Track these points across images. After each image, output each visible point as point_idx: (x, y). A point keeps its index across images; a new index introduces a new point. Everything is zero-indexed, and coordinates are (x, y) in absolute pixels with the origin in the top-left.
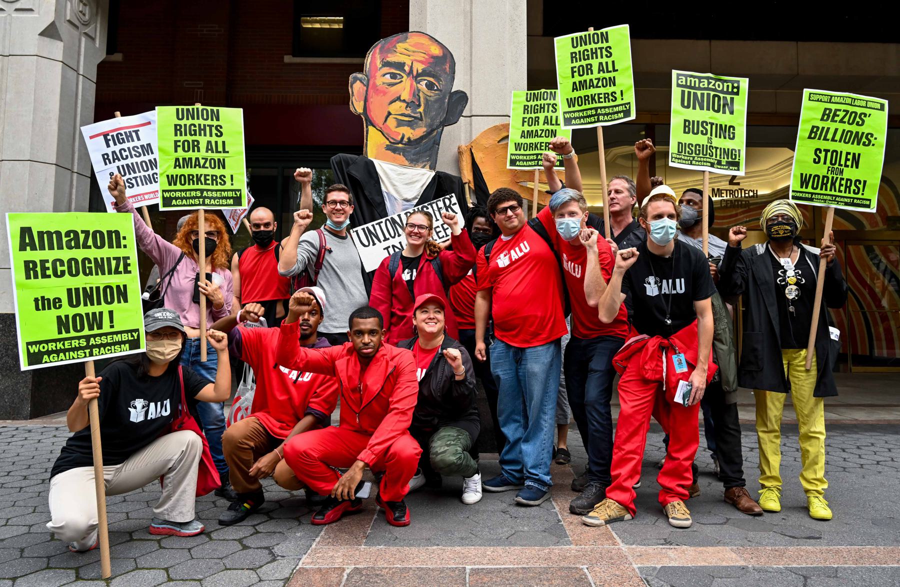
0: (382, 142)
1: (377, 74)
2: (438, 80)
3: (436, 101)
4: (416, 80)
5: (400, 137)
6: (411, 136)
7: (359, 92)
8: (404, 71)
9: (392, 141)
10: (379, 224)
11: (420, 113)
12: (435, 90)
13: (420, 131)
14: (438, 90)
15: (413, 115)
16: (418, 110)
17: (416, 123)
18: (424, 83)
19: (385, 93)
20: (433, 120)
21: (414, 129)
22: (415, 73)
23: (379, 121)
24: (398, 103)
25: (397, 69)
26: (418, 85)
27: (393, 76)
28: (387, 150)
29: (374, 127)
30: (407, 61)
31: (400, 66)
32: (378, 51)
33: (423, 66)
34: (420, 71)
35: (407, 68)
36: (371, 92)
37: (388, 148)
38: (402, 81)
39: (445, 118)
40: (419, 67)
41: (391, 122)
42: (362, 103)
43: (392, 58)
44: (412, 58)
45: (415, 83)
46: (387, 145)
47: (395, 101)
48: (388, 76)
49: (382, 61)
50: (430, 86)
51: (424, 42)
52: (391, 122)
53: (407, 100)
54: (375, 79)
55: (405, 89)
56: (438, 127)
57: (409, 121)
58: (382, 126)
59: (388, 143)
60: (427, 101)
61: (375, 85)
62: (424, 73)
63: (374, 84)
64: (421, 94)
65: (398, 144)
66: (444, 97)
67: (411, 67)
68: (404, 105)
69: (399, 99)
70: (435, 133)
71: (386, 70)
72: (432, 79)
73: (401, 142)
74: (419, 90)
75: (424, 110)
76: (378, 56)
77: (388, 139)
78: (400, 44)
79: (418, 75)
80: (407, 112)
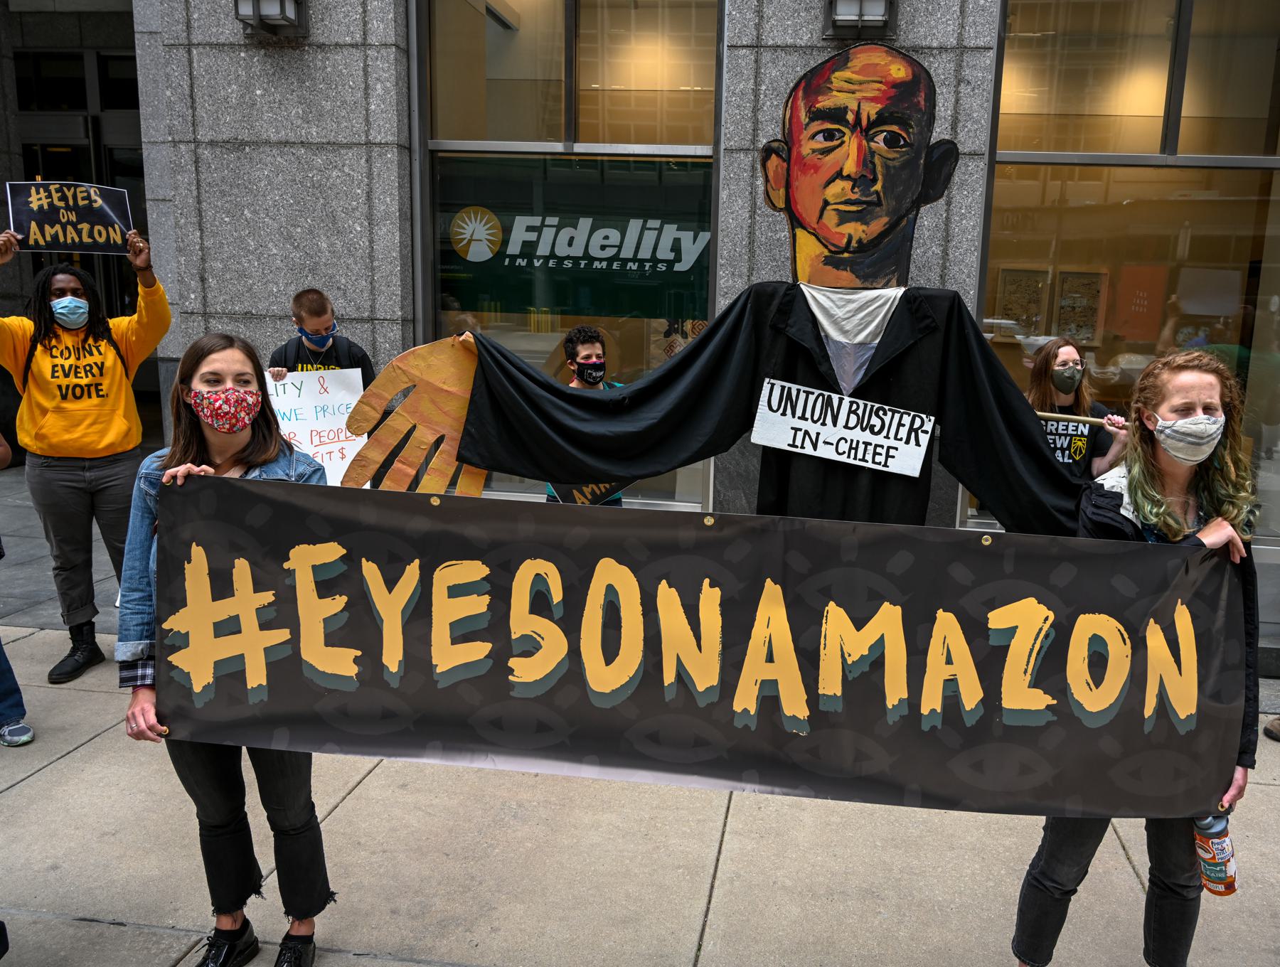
0: (818, 252)
1: (801, 137)
2: (904, 124)
3: (904, 166)
4: (866, 135)
6: (863, 236)
7: (776, 172)
8: (844, 122)
9: (833, 249)
10: (808, 393)
11: (877, 193)
12: (902, 147)
13: (878, 225)
14: (906, 145)
15: (864, 199)
19: (816, 168)
21: (867, 223)
22: (864, 122)
23: (810, 216)
25: (833, 122)
26: (872, 144)
27: (829, 135)
28: (825, 264)
29: (805, 228)
30: (850, 102)
31: (837, 115)
32: (801, 94)
33: (879, 106)
34: (873, 117)
35: (850, 117)
36: (795, 171)
37: (828, 261)
38: (843, 143)
39: (920, 194)
40: (871, 110)
41: (830, 218)
42: (782, 191)
43: (825, 103)
44: (858, 95)
45: (864, 142)
46: (826, 257)
48: (820, 137)
49: (809, 111)
50: (892, 141)
51: (877, 61)
52: (830, 218)
53: (853, 176)
54: (800, 146)
55: (848, 155)
56: (908, 211)
57: (858, 211)
58: (815, 226)
59: (826, 253)
60: (886, 167)
61: (801, 157)
62: (881, 119)
64: (877, 160)
66: (918, 157)
67: (858, 115)
68: (848, 185)
69: (839, 175)
70: (904, 223)
71: (817, 126)
72: (895, 128)
73: (846, 249)
74: (873, 153)
75: (883, 187)
76: (801, 104)
77: (826, 247)
78: (837, 74)
79: (871, 124)
80: (854, 197)
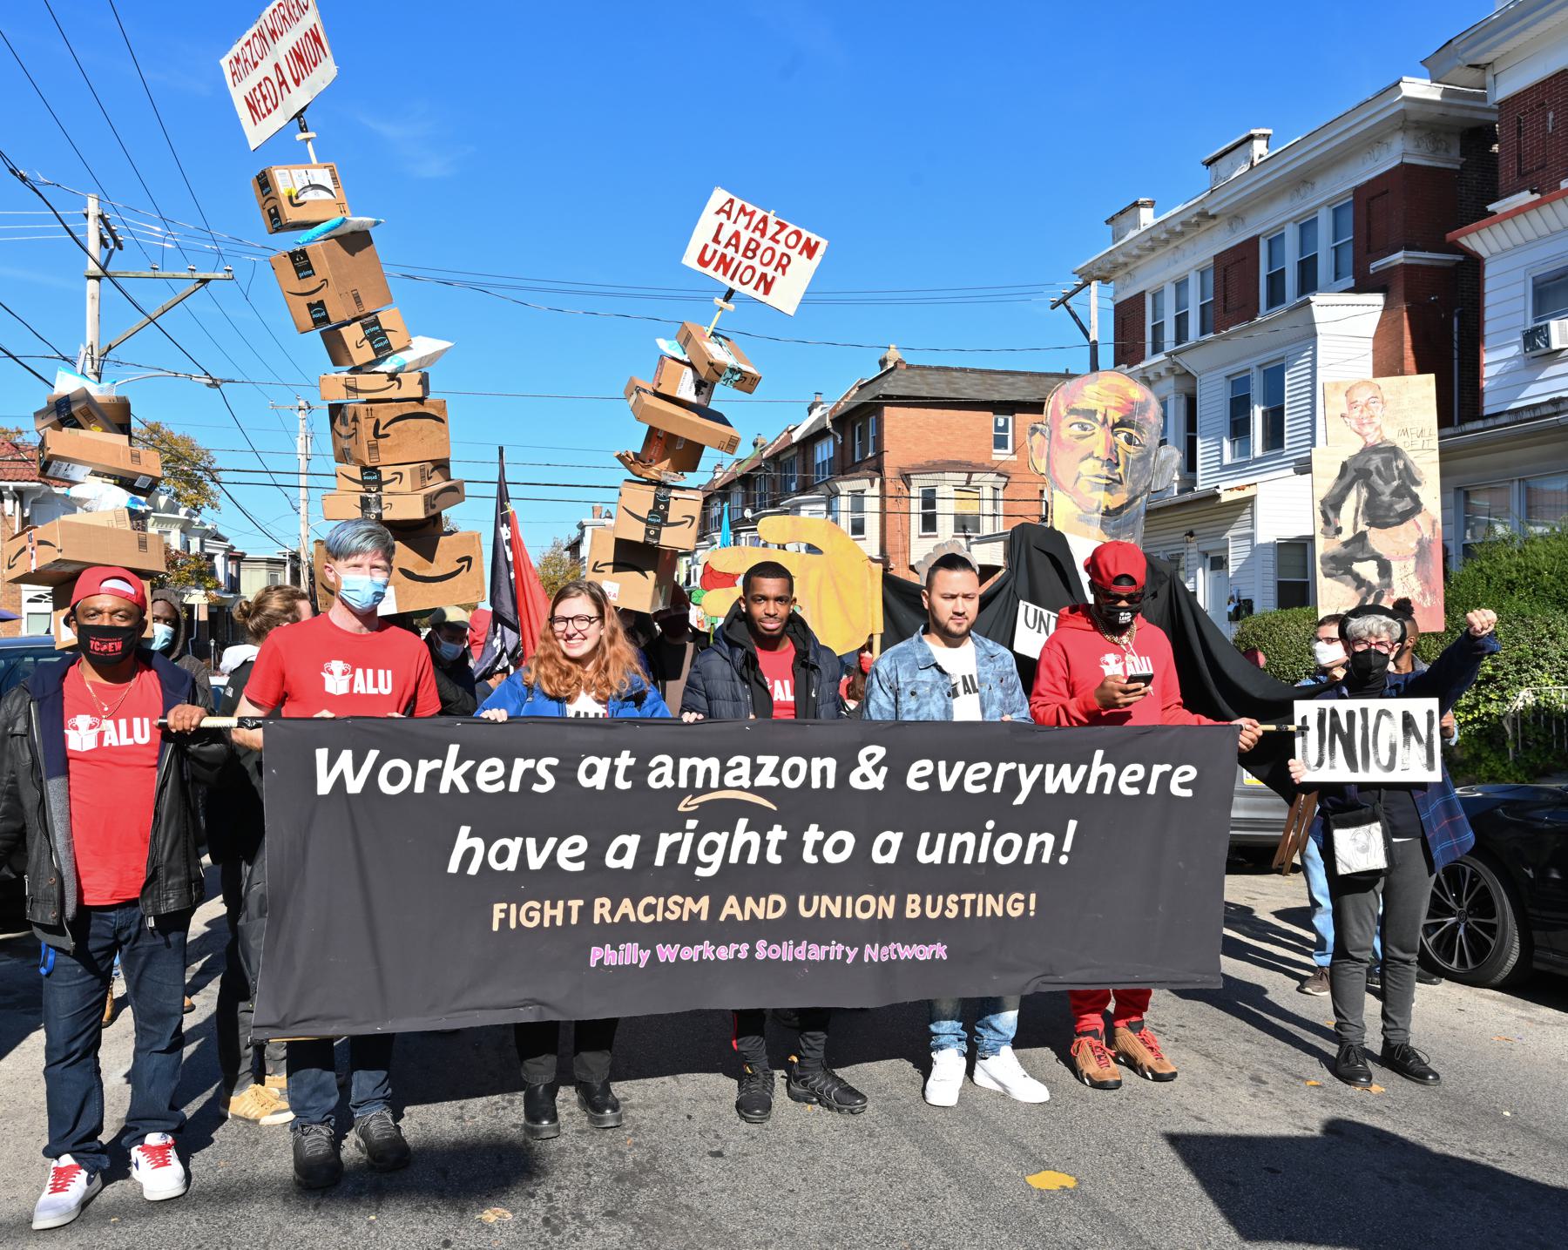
1: (1061, 425)
5: (1096, 505)
6: (1109, 504)
8: (1096, 421)
14: (1140, 445)
16: (1117, 471)
17: (1115, 487)
18: (1122, 436)
20: (1135, 482)
22: (1110, 423)
24: (1090, 461)
31: (1091, 414)
34: (1117, 421)
40: (1115, 416)
45: (1111, 436)
46: (1079, 515)
47: (1086, 459)
50: (1129, 440)
59: (1080, 512)
63: (1059, 436)
64: (1119, 450)
65: (1093, 513)
67: (1105, 416)
71: (1073, 418)
74: (1117, 445)
79: (1115, 426)
